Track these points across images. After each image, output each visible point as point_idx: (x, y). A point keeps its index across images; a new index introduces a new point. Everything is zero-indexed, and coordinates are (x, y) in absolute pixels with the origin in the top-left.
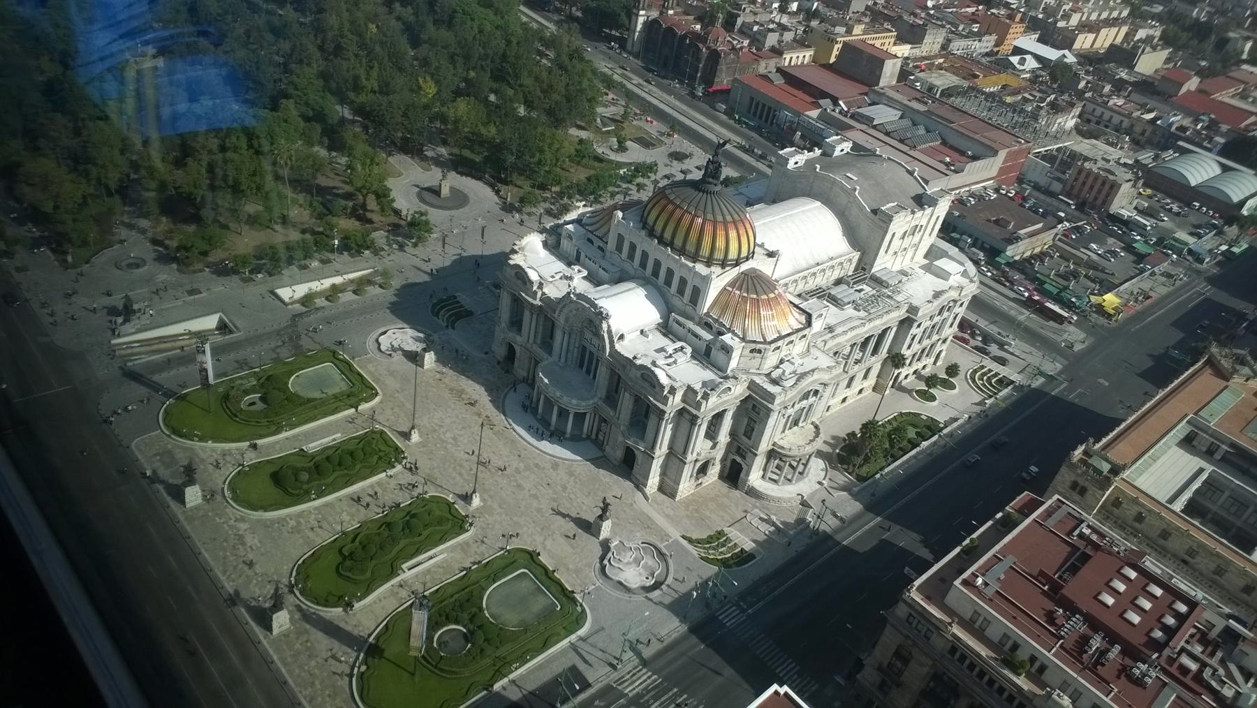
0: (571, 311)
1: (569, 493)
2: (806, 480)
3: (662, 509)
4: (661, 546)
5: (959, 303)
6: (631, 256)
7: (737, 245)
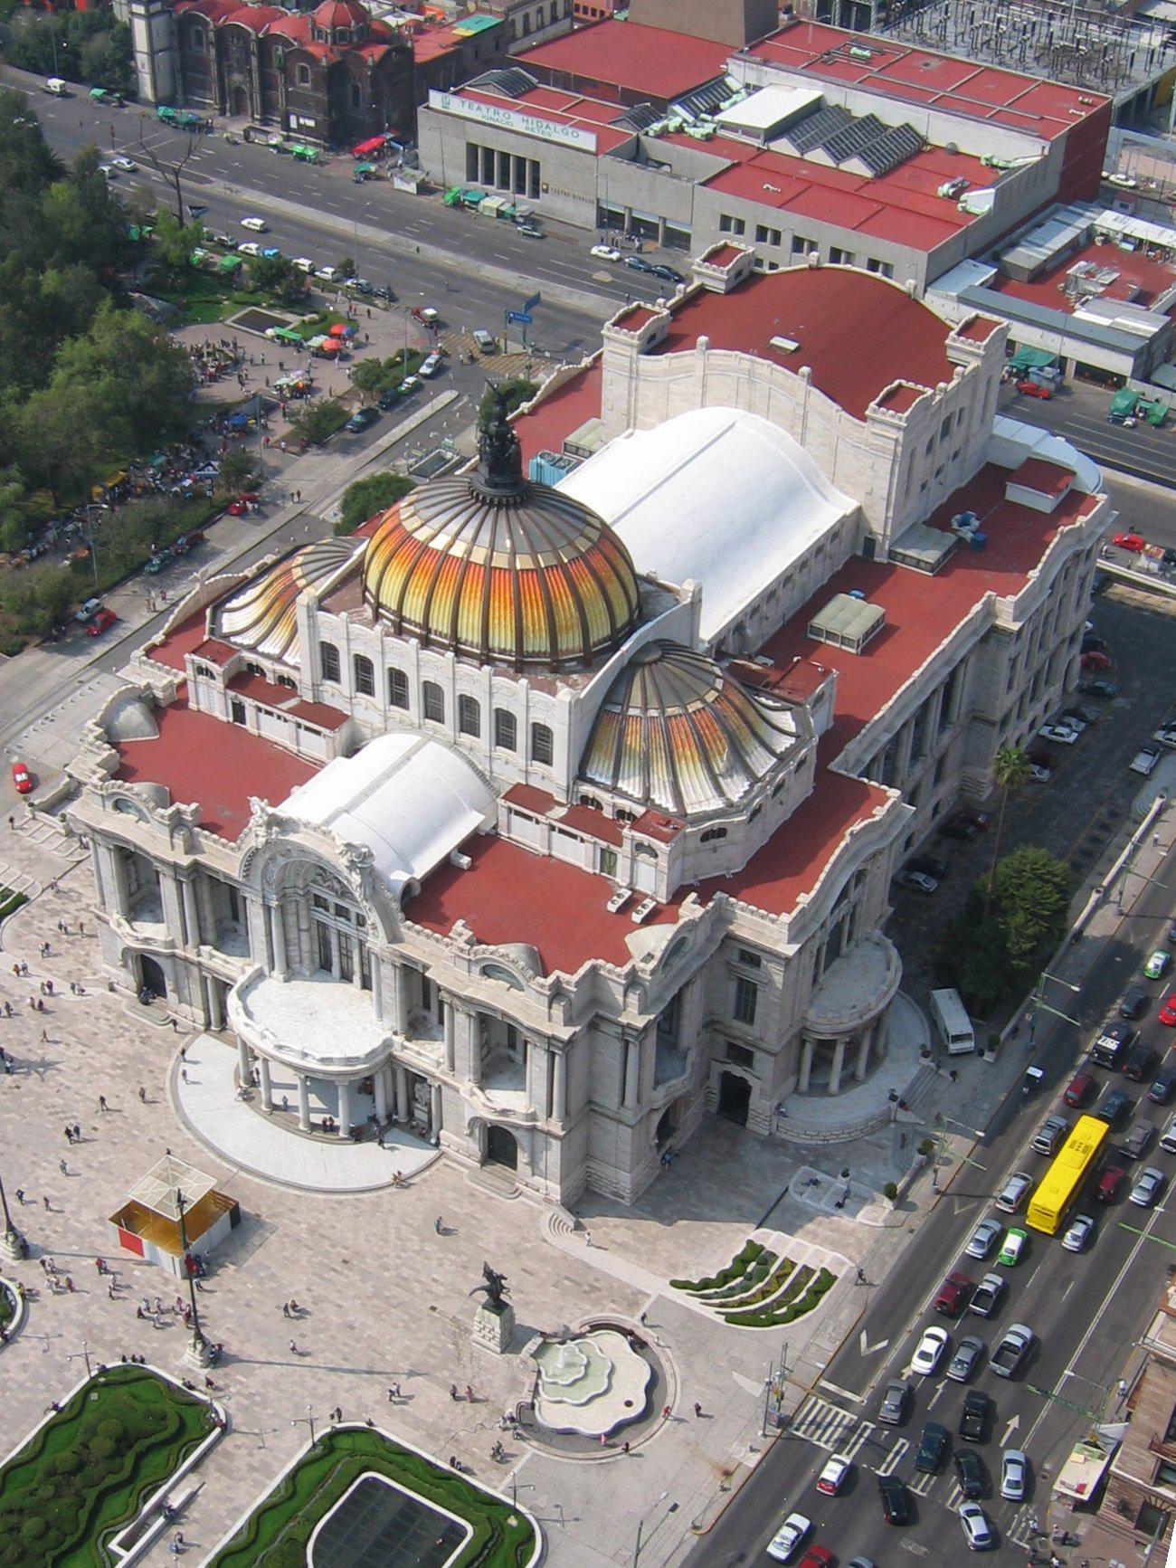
0: (272, 859)
1: (397, 1267)
2: (887, 1064)
3: (606, 1234)
4: (632, 1321)
5: (1083, 556)
6: (365, 686)
7: (602, 605)
